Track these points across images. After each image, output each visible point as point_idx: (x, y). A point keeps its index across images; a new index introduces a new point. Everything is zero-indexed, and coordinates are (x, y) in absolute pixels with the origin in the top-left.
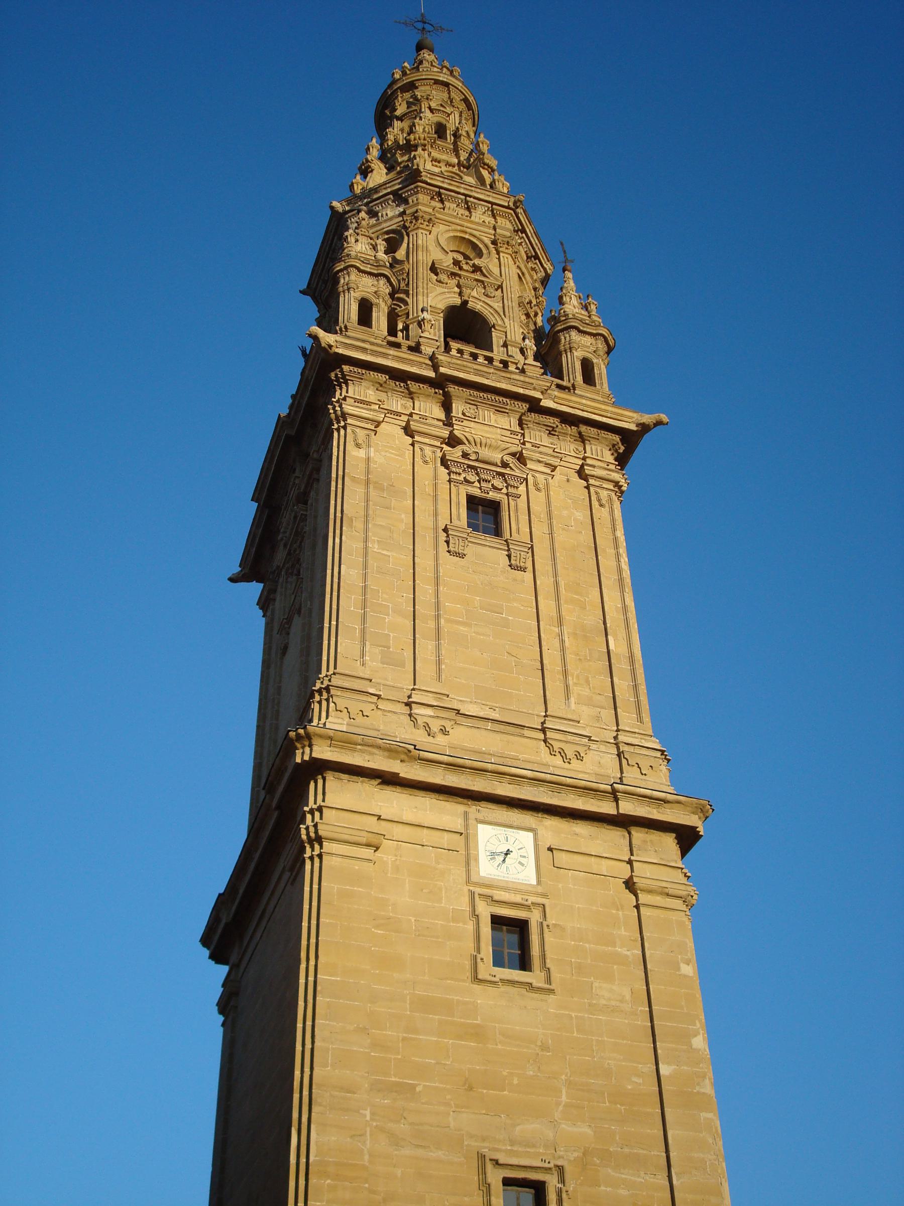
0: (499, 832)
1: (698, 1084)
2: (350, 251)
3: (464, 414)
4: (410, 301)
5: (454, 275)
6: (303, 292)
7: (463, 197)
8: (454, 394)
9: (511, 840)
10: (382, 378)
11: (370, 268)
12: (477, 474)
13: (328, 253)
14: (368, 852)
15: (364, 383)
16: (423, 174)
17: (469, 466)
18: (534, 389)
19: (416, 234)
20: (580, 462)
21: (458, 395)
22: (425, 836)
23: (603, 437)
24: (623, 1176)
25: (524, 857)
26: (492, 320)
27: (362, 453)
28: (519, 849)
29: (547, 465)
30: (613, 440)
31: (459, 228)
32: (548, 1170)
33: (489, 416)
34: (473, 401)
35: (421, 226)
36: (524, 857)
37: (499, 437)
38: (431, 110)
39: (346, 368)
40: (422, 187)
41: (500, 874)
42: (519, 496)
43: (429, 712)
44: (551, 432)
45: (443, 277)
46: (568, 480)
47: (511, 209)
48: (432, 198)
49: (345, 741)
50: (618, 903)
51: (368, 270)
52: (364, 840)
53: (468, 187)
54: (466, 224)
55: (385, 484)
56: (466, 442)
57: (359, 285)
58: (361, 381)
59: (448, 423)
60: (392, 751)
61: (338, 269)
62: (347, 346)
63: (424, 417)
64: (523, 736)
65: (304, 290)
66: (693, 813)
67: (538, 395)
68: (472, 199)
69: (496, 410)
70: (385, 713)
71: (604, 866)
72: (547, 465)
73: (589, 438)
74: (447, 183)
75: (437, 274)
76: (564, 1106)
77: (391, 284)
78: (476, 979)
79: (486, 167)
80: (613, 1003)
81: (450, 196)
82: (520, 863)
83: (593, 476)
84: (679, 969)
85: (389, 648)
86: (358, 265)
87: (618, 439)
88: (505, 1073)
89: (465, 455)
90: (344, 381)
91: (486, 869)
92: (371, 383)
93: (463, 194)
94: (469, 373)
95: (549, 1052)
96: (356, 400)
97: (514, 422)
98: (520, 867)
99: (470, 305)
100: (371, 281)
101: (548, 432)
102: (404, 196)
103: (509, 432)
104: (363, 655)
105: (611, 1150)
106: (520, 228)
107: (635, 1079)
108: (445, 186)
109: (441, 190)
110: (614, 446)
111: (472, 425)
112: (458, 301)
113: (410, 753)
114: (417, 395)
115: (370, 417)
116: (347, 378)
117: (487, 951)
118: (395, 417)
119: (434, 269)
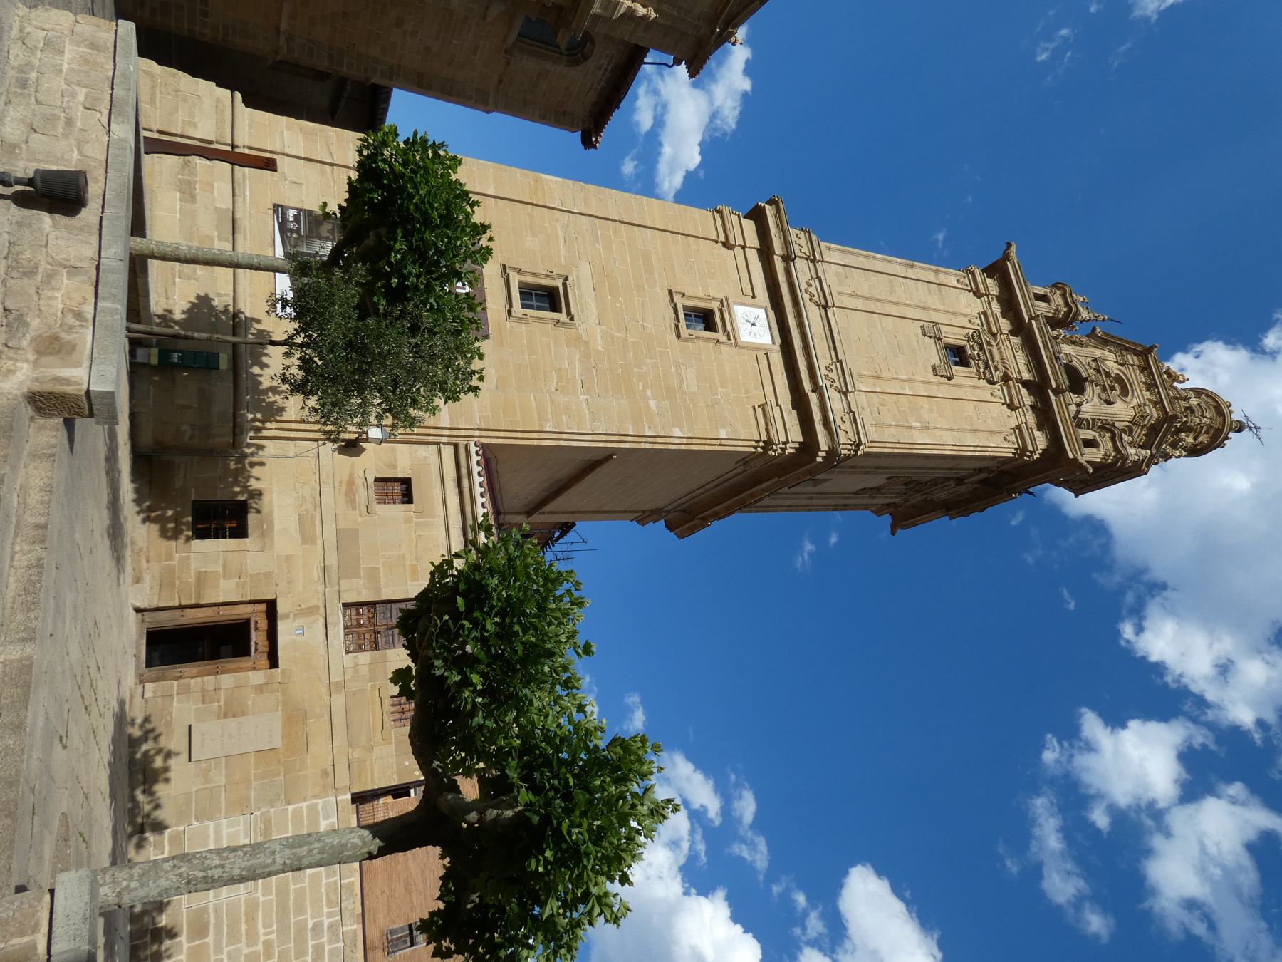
1: (650, 427)
14: (722, 238)
18: (1056, 381)
29: (1011, 399)
32: (569, 312)
33: (1022, 359)
38: (1198, 405)
60: (787, 244)
62: (1014, 267)
71: (769, 388)
72: (1011, 399)
82: (750, 333)
89: (989, 344)
97: (1026, 376)
98: (748, 331)
107: (641, 384)
113: (788, 259)
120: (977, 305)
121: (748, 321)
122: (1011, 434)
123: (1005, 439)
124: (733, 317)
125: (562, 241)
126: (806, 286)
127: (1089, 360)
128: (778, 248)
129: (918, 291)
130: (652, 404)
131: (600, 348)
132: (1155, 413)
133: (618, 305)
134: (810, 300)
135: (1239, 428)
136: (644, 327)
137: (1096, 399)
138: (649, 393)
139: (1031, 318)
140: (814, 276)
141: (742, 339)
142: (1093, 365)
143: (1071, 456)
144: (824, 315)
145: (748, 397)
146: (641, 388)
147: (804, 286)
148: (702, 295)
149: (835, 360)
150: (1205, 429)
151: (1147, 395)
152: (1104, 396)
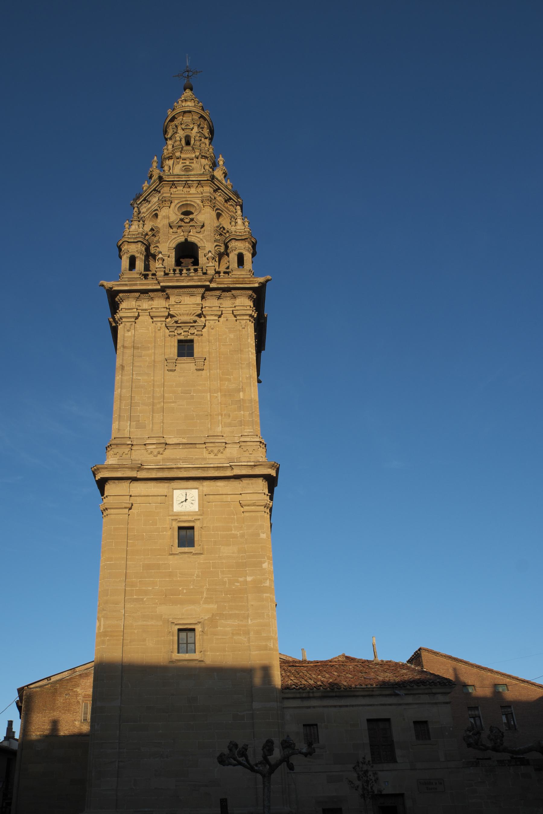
0: (183, 492)
2: (125, 233)
8: (170, 293)
10: (137, 294)
11: (133, 240)
15: (130, 299)
16: (164, 177)
17: (178, 327)
18: (205, 281)
21: (172, 293)
22: (150, 499)
23: (244, 294)
24: (228, 623)
25: (194, 500)
26: (199, 245)
27: (129, 334)
28: (191, 497)
30: (249, 294)
31: (184, 199)
32: (196, 624)
33: (187, 300)
34: (179, 294)
35: (165, 205)
36: (194, 500)
37: (192, 309)
38: (183, 130)
39: (121, 295)
40: (165, 184)
41: (183, 509)
43: (154, 446)
46: (227, 320)
47: (209, 180)
49: (113, 468)
50: (235, 512)
51: (132, 241)
52: (124, 506)
53: (187, 177)
54: (188, 196)
55: (140, 345)
56: (176, 316)
57: (129, 250)
58: (128, 299)
61: (120, 244)
62: (118, 285)
63: (157, 308)
64: (196, 448)
66: (269, 468)
67: (208, 283)
69: (190, 295)
70: (135, 451)
71: (229, 498)
73: (237, 296)
74: (176, 178)
75: (172, 229)
76: (205, 598)
77: (145, 244)
79: (203, 157)
80: (229, 555)
81: (179, 183)
82: (192, 503)
83: (238, 315)
84: (259, 536)
86: (127, 240)
87: (251, 293)
88: (180, 589)
89: (176, 322)
90: (122, 300)
91: (177, 508)
92: (133, 299)
94: (173, 282)
95: (199, 578)
96: (126, 309)
97: (198, 299)
99: (189, 239)
100: (135, 245)
101: (217, 298)
102: (158, 190)
103: (196, 305)
105: (224, 613)
106: (217, 188)
107: (236, 584)
108: (176, 179)
109: (174, 182)
110: (250, 296)
111: (178, 306)
114: (155, 298)
115: (132, 315)
116: (122, 299)
118: (145, 312)
120: (144, 318)
121: (182, 502)
122: (240, 323)
123: (244, 328)
124: (183, 514)
125: (145, 622)
126: (151, 455)
127: (171, 230)
128: (133, 474)
129: (141, 366)
130: (249, 579)
131: (216, 606)
132: (207, 190)
133: (185, 591)
134: (162, 454)
136: (198, 576)
137: (200, 236)
138: (241, 579)
140: (143, 447)
141: (197, 510)
142: (175, 230)
143: (256, 285)
144: (172, 447)
145: (236, 514)
146: (239, 584)
147: (151, 458)
148: (169, 533)
149: (204, 446)
150: (200, 130)
151: (193, 190)
152: (198, 229)
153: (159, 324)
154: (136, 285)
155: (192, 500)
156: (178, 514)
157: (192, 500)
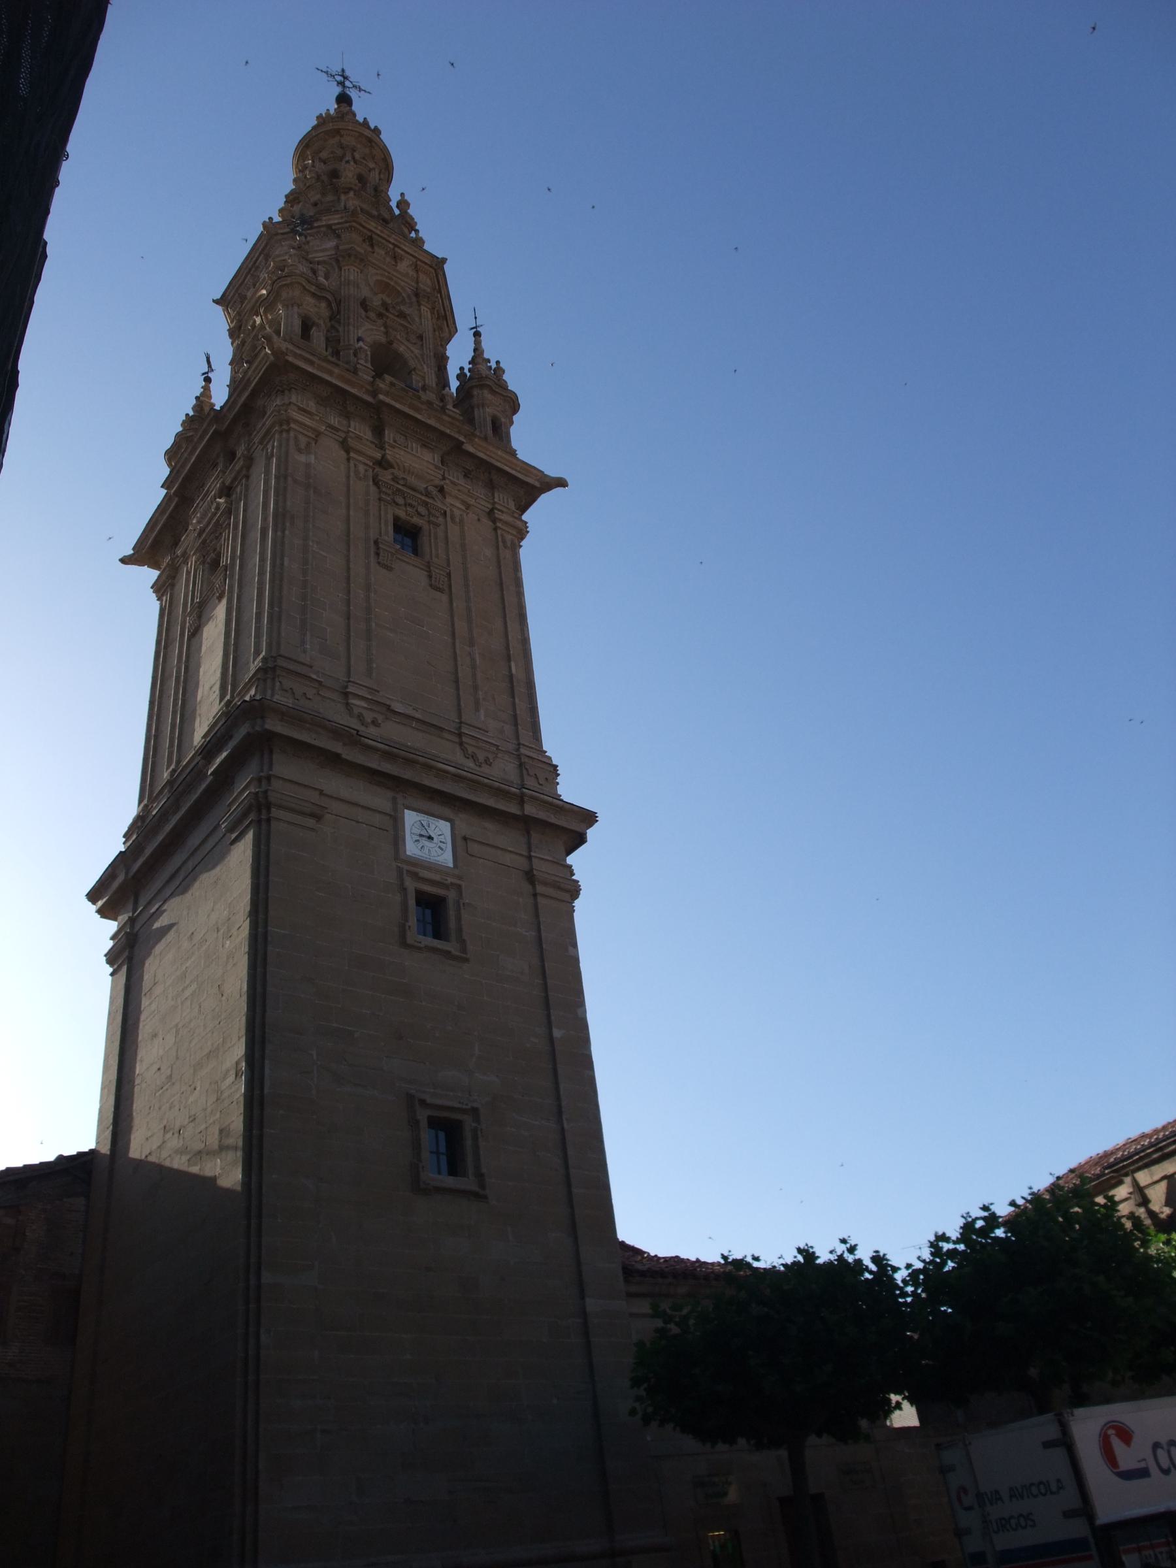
3: (395, 441)
4: (341, 329)
5: (380, 315)
6: (216, 302)
7: (391, 246)
9: (433, 827)
12: (404, 498)
13: (250, 270)
14: (311, 822)
17: (398, 490)
19: (349, 269)
20: (490, 506)
25: (443, 843)
27: (302, 458)
29: (463, 502)
34: (402, 431)
36: (443, 843)
41: (423, 855)
42: (438, 525)
44: (467, 475)
45: (372, 315)
46: (479, 520)
48: (364, 241)
56: (395, 466)
59: (382, 448)
65: (217, 299)
68: (399, 251)
75: (366, 311)
78: (404, 944)
79: (407, 225)
82: (440, 847)
85: (326, 640)
89: (395, 479)
91: (411, 848)
93: (393, 244)
97: (437, 458)
98: (440, 852)
104: (303, 642)
108: (378, 232)
112: (383, 340)
117: (413, 921)
119: (364, 304)
135: (344, 99)
139: (374, 394)
141: (451, 865)
153: (361, 468)
154: (331, 373)
155: (441, 842)
156: (415, 862)
157: (441, 842)
